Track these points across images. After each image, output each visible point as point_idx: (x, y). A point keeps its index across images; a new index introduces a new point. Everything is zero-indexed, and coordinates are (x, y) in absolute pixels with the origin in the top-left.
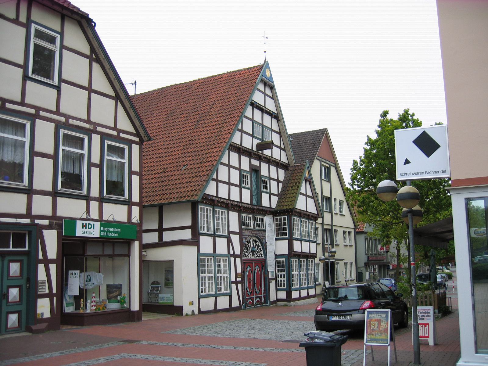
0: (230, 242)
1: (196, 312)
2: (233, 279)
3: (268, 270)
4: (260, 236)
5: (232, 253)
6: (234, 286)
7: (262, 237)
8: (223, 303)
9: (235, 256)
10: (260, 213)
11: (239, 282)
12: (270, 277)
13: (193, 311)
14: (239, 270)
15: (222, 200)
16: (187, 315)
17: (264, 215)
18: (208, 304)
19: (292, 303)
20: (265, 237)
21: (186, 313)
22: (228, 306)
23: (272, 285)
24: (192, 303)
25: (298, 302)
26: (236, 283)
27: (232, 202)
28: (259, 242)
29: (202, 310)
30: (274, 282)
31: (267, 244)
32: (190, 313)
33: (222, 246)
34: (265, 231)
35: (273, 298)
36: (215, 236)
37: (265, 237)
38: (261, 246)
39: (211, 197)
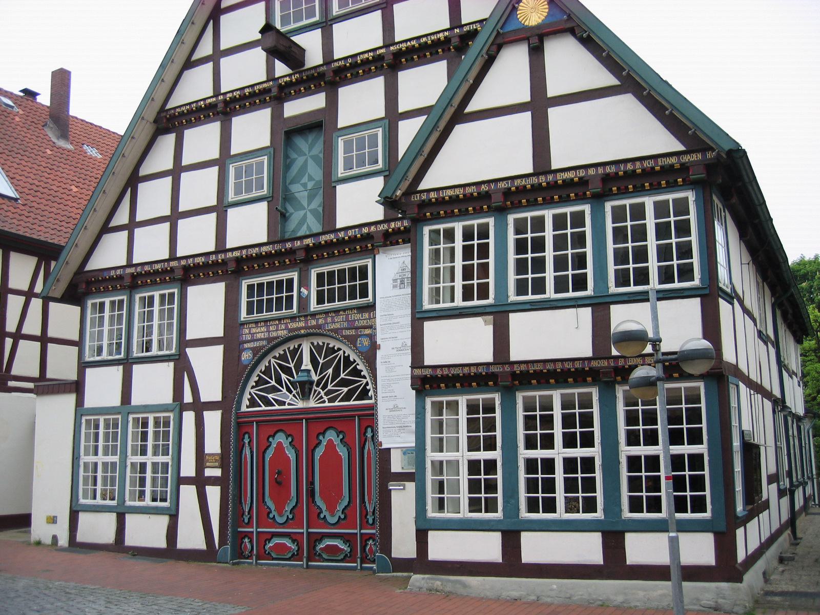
0: (182, 368)
1: (63, 541)
2: (188, 469)
3: (381, 444)
4: (336, 331)
5: (188, 398)
6: (188, 493)
7: (348, 332)
8: (146, 531)
9: (200, 407)
10: (323, 257)
11: (213, 481)
12: (397, 465)
13: (55, 538)
14: (213, 445)
15: (147, 268)
16: (39, 543)
17: (371, 252)
18: (98, 528)
19: (417, 579)
20: (370, 327)
21: (38, 539)
22: (162, 543)
23: (403, 501)
24: (53, 520)
25: (474, 582)
26: (200, 482)
27: (183, 262)
28: (344, 348)
29: (80, 537)
30: (411, 486)
31: (379, 354)
32: (48, 541)
33: (154, 384)
34: (371, 307)
35: (403, 544)
36: (130, 361)
37: (370, 327)
38: (358, 361)
39: (113, 273)
